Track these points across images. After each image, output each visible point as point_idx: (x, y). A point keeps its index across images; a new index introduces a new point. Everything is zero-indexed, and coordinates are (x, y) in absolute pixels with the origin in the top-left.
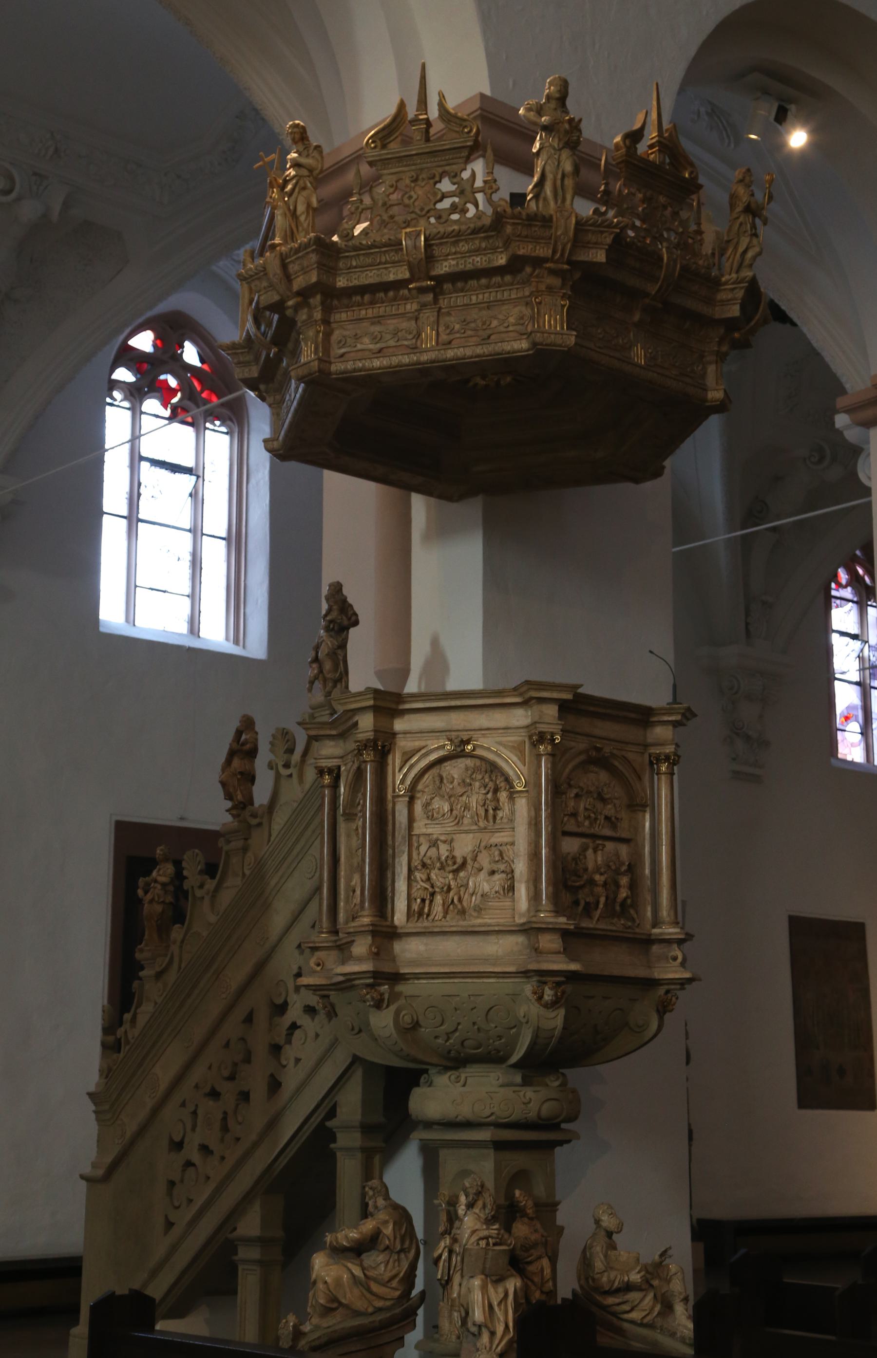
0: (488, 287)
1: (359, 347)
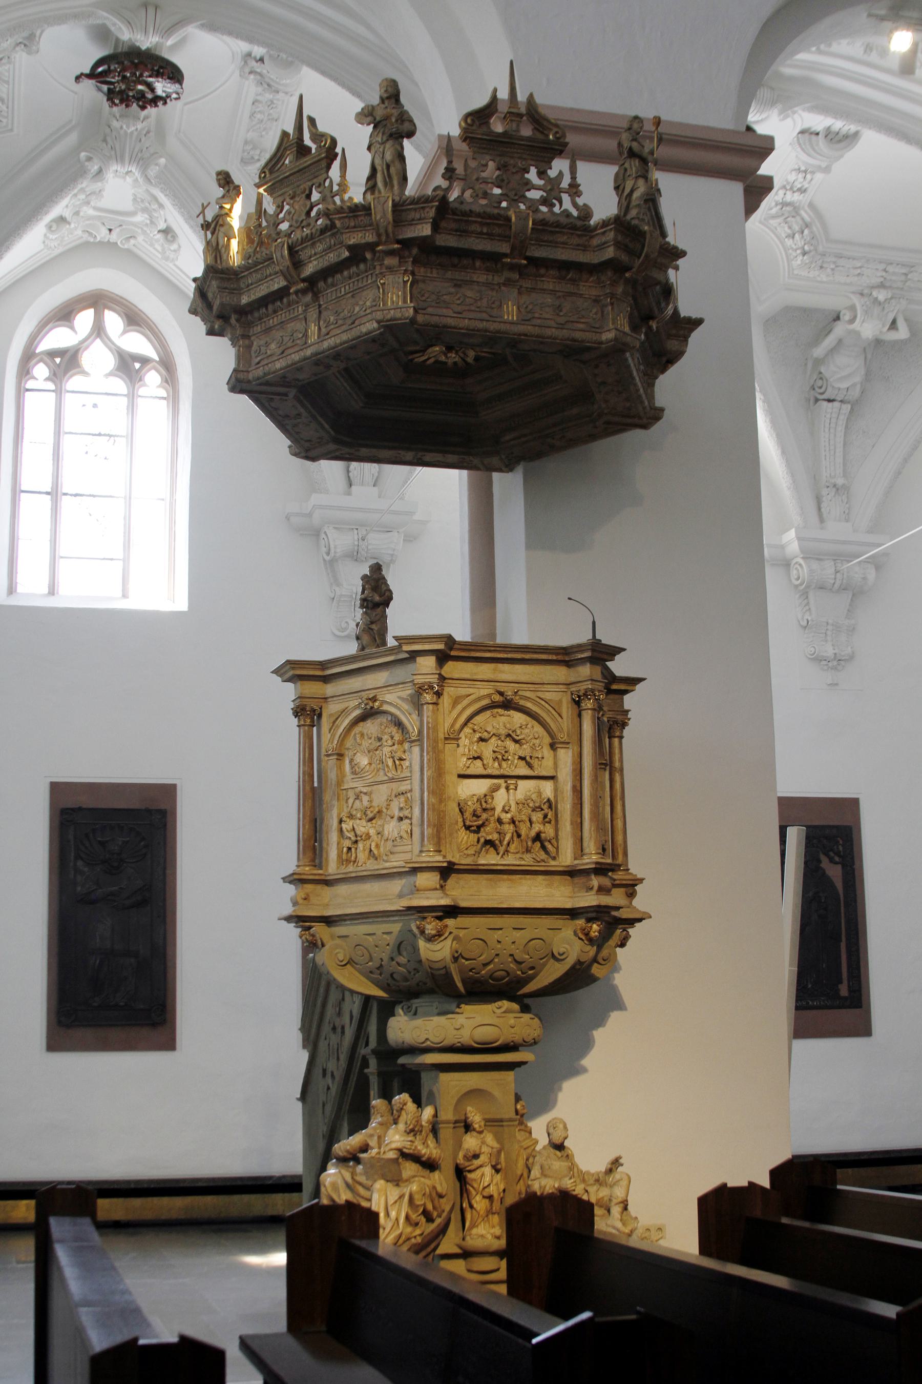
0: (350, 278)
1: (269, 353)
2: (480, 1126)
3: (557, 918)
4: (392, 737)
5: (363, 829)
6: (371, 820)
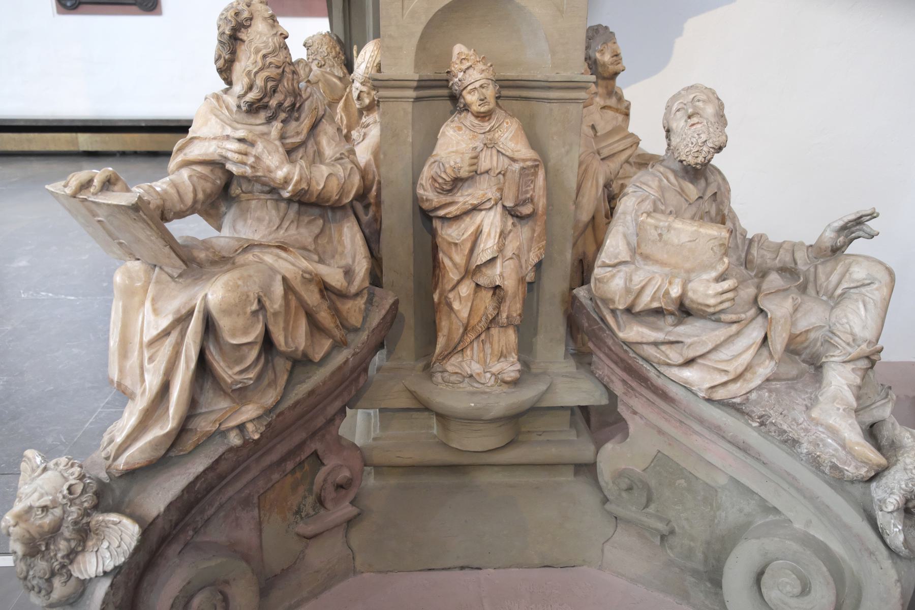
2: (483, 100)
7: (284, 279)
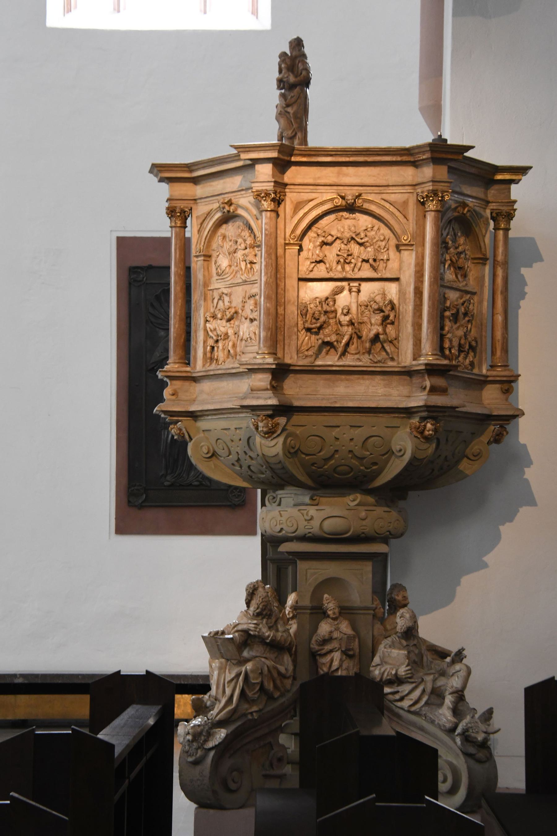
2: (334, 613)
3: (394, 417)
4: (245, 241)
5: (223, 329)
6: (229, 320)
7: (267, 666)
